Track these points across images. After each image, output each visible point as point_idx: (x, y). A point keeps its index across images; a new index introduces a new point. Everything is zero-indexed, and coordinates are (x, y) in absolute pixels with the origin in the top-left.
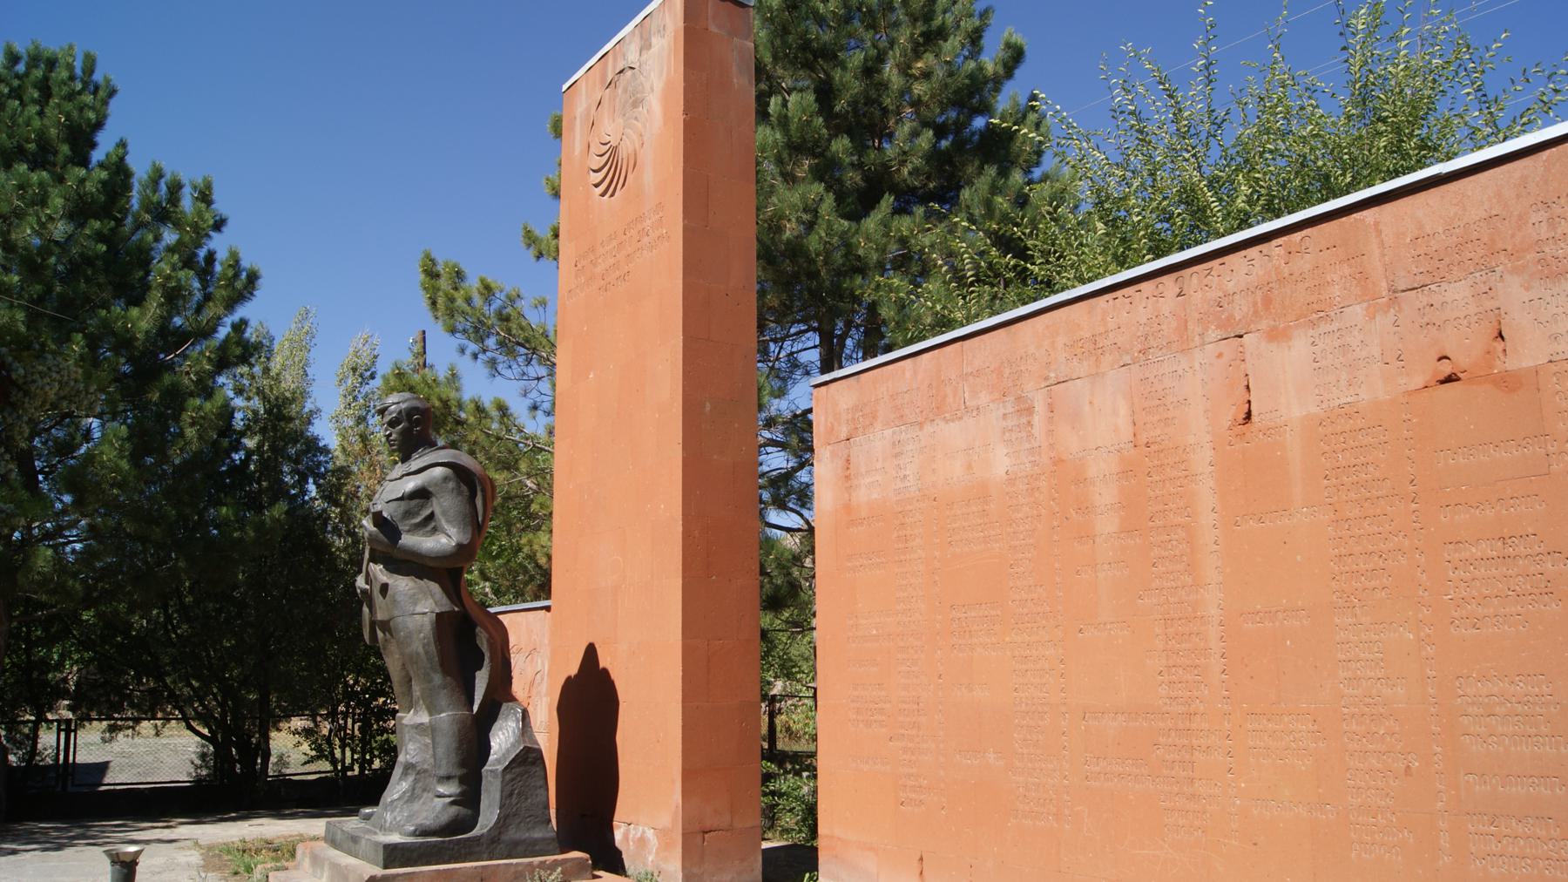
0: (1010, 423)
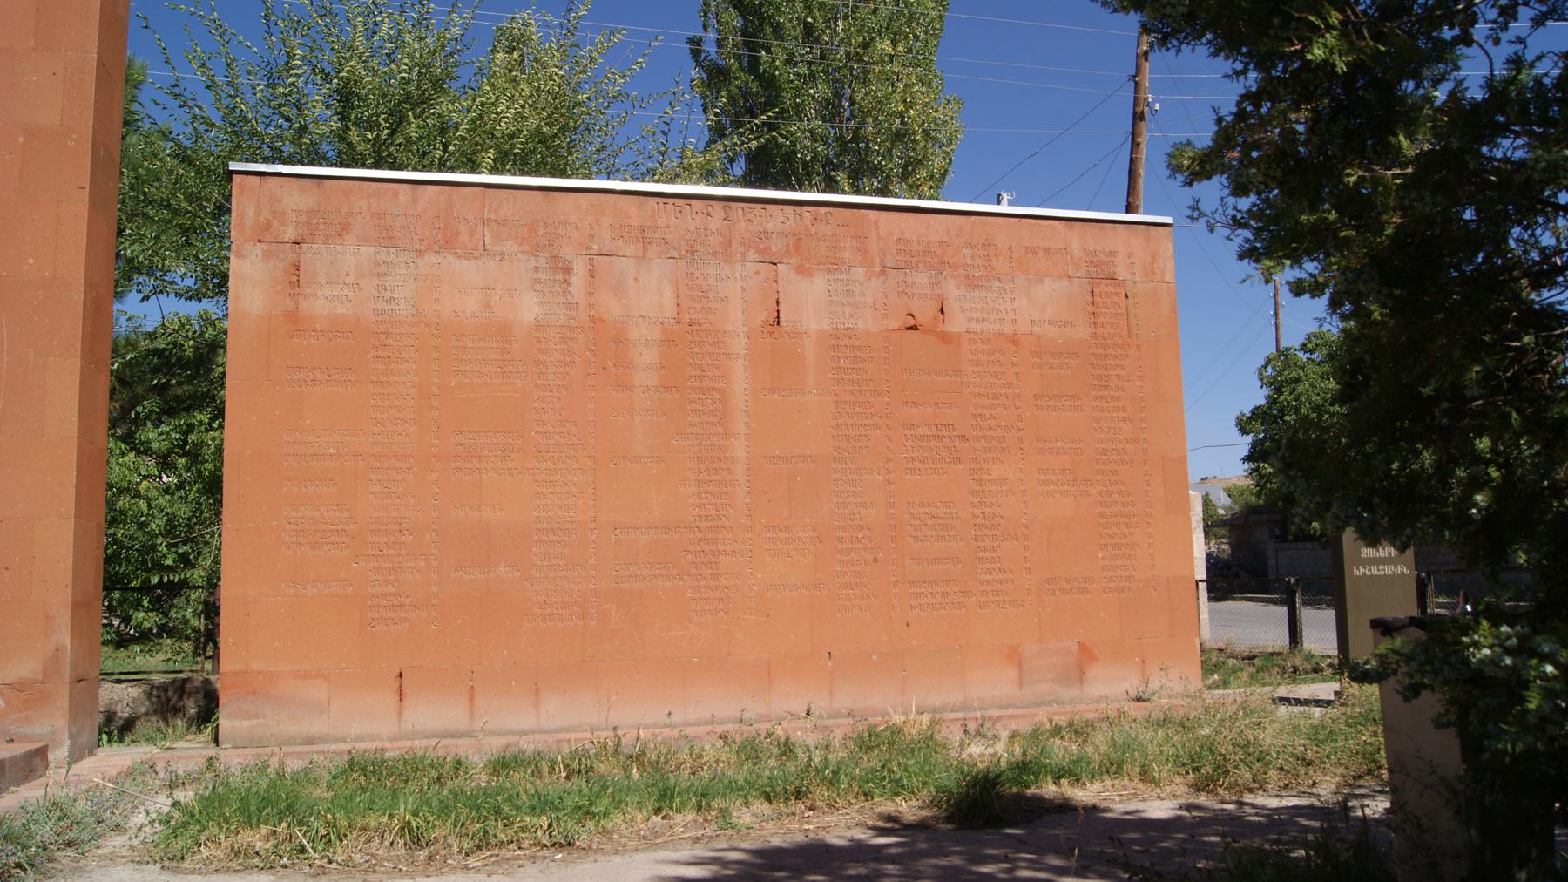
0: (540, 276)
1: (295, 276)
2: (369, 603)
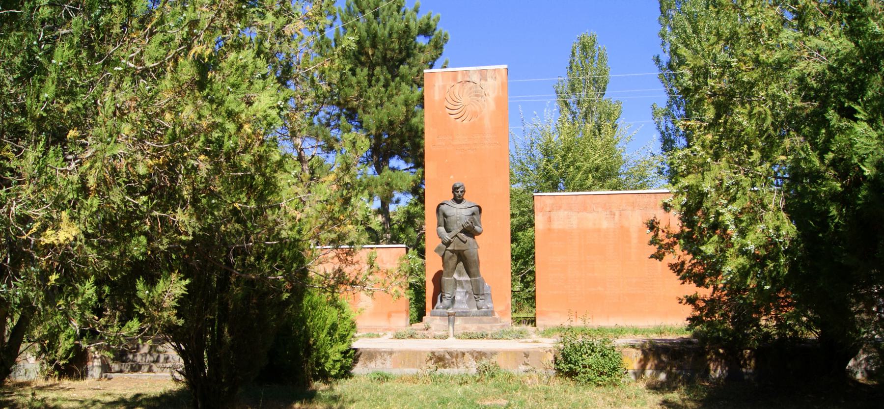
1: (550, 220)
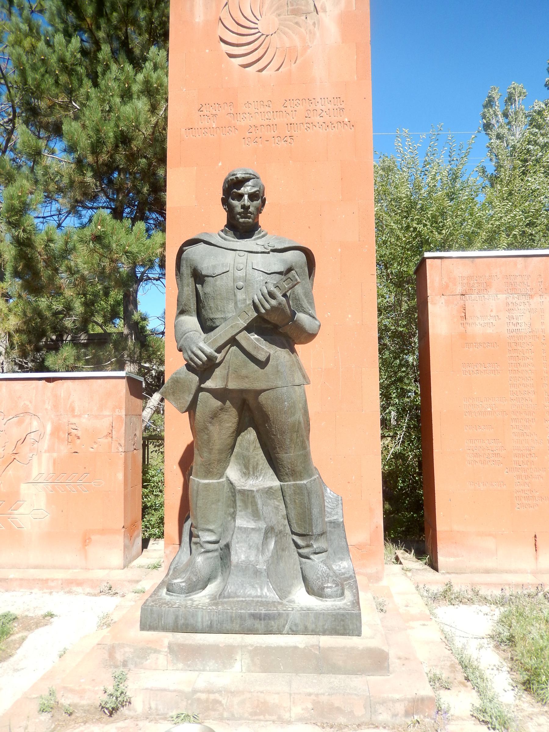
2: (515, 495)
